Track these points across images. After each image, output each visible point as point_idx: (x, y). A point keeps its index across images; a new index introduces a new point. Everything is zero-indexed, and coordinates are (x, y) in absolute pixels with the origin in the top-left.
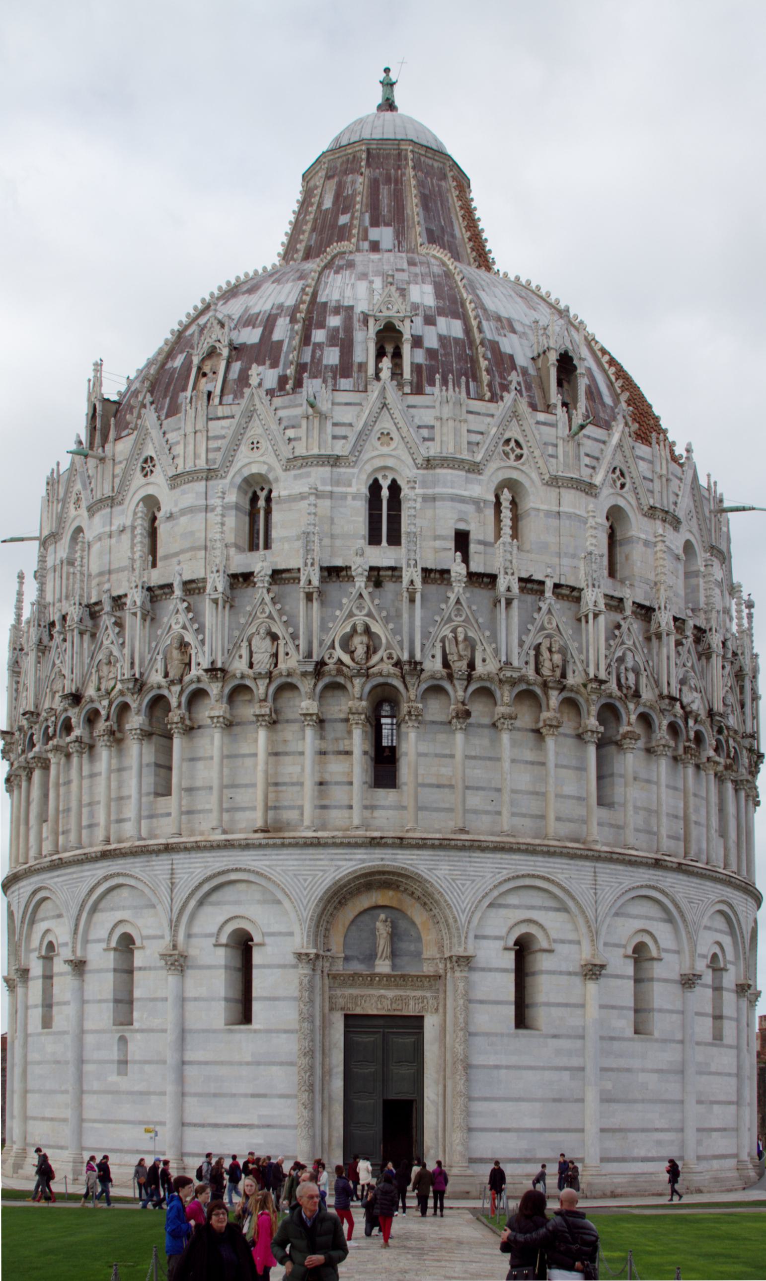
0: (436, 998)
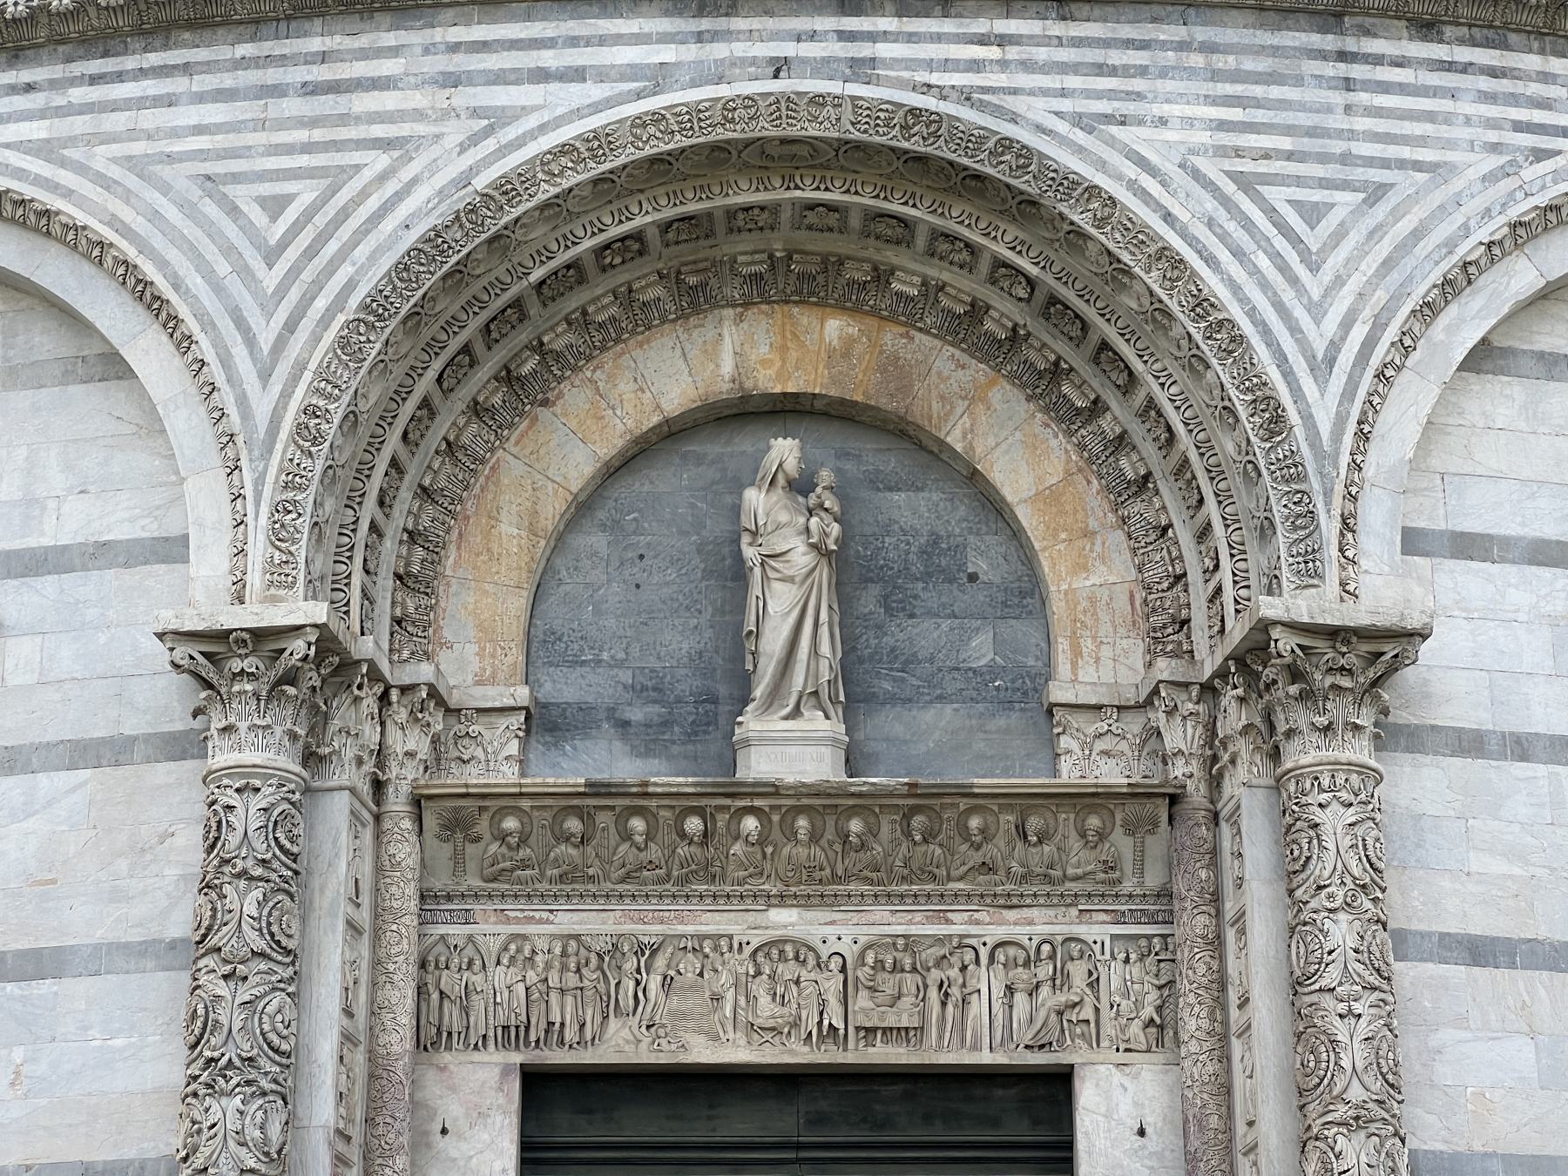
0: (1161, 954)
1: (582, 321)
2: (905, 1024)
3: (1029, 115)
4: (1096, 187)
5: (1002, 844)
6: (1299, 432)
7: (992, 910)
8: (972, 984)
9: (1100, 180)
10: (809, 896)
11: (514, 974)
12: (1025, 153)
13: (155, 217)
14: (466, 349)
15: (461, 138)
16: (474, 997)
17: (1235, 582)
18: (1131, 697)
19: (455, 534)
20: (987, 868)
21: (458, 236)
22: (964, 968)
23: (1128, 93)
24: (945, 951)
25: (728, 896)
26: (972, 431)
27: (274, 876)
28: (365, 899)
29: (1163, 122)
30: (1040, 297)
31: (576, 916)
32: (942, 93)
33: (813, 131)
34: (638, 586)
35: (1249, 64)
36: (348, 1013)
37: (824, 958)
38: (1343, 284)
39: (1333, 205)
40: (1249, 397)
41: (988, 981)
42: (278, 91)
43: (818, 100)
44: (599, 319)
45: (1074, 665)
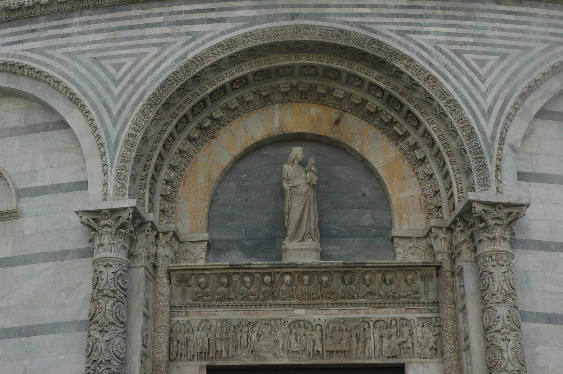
1: (226, 108)
2: (344, 349)
3: (382, 31)
4: (405, 55)
5: (377, 285)
6: (480, 137)
7: (374, 309)
8: (367, 335)
9: (406, 52)
10: (309, 304)
11: (203, 334)
12: (380, 44)
13: (77, 72)
14: (185, 116)
15: (184, 42)
16: (190, 342)
17: (458, 191)
18: (421, 234)
19: (182, 182)
20: (371, 293)
21: (182, 75)
22: (364, 329)
23: (415, 23)
24: (358, 324)
25: (280, 305)
26: (362, 144)
27: (117, 296)
28: (150, 307)
29: (428, 33)
30: (386, 96)
31: (225, 313)
32: (352, 24)
33: (306, 38)
34: (247, 200)
35: (457, 14)
36: (144, 346)
37: (314, 326)
38: (493, 87)
39: (489, 60)
40: (461, 126)
41: (373, 335)
42: (120, 29)
43: (308, 27)
44: (232, 107)
45: (401, 223)
